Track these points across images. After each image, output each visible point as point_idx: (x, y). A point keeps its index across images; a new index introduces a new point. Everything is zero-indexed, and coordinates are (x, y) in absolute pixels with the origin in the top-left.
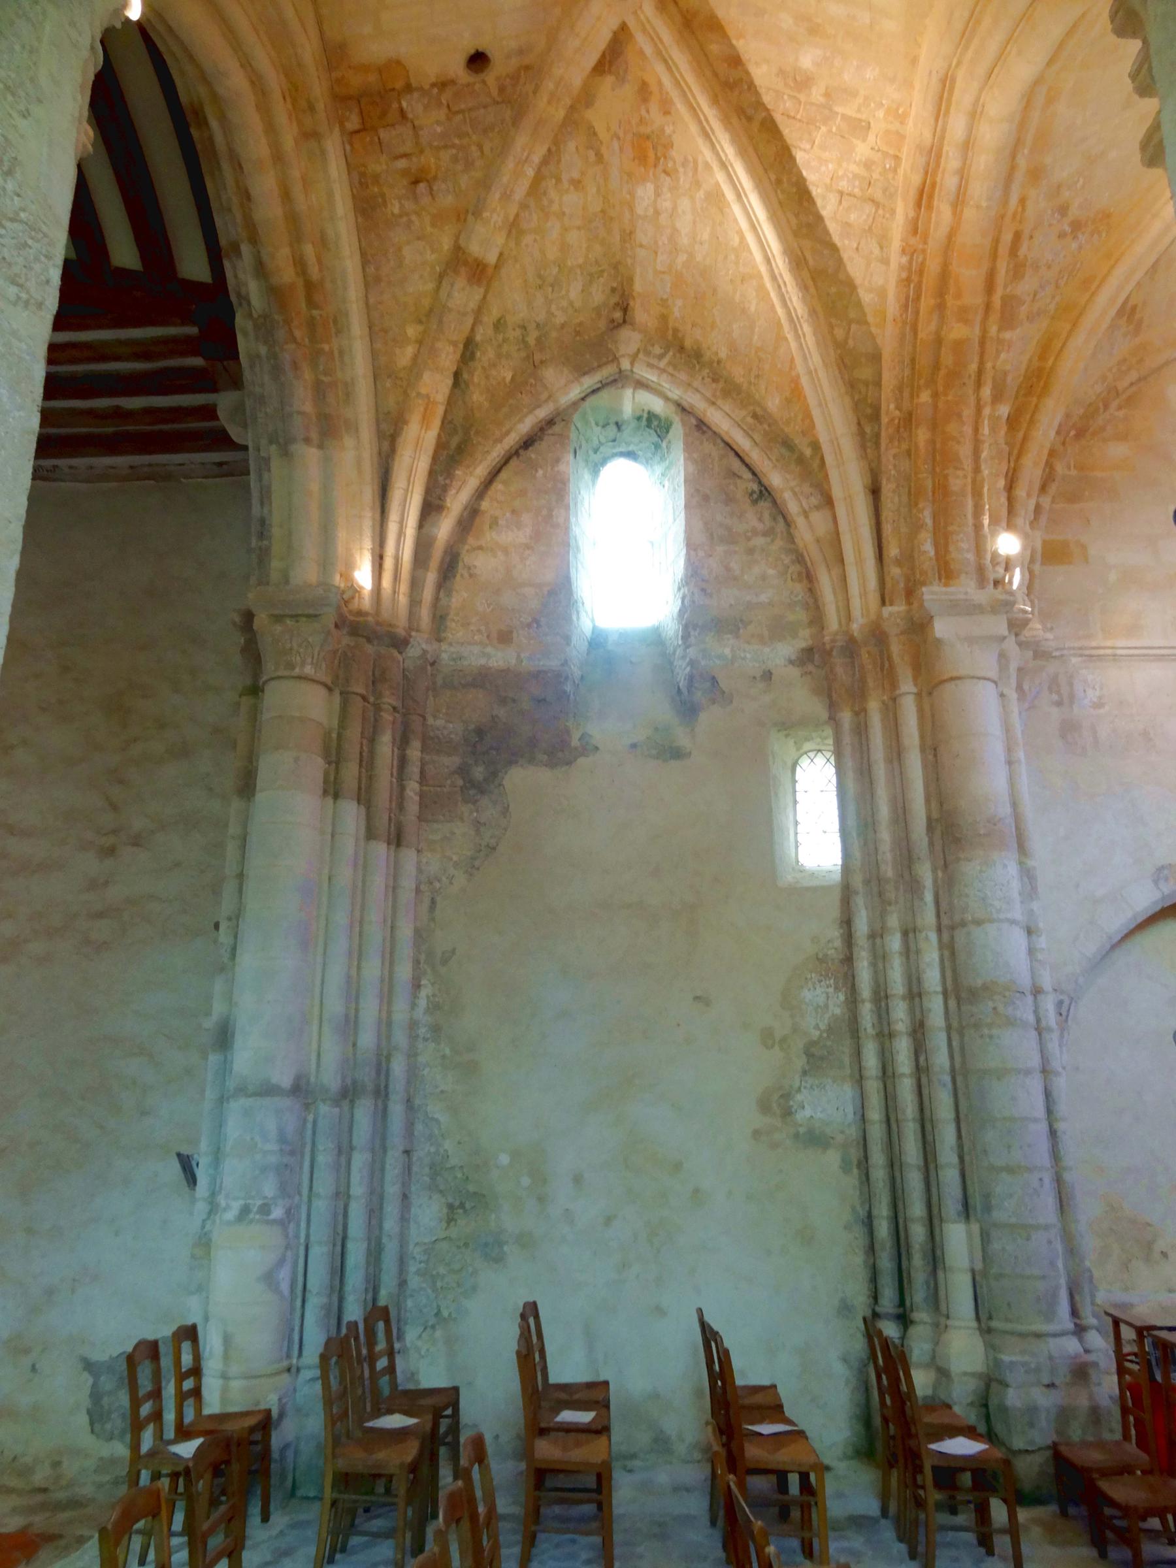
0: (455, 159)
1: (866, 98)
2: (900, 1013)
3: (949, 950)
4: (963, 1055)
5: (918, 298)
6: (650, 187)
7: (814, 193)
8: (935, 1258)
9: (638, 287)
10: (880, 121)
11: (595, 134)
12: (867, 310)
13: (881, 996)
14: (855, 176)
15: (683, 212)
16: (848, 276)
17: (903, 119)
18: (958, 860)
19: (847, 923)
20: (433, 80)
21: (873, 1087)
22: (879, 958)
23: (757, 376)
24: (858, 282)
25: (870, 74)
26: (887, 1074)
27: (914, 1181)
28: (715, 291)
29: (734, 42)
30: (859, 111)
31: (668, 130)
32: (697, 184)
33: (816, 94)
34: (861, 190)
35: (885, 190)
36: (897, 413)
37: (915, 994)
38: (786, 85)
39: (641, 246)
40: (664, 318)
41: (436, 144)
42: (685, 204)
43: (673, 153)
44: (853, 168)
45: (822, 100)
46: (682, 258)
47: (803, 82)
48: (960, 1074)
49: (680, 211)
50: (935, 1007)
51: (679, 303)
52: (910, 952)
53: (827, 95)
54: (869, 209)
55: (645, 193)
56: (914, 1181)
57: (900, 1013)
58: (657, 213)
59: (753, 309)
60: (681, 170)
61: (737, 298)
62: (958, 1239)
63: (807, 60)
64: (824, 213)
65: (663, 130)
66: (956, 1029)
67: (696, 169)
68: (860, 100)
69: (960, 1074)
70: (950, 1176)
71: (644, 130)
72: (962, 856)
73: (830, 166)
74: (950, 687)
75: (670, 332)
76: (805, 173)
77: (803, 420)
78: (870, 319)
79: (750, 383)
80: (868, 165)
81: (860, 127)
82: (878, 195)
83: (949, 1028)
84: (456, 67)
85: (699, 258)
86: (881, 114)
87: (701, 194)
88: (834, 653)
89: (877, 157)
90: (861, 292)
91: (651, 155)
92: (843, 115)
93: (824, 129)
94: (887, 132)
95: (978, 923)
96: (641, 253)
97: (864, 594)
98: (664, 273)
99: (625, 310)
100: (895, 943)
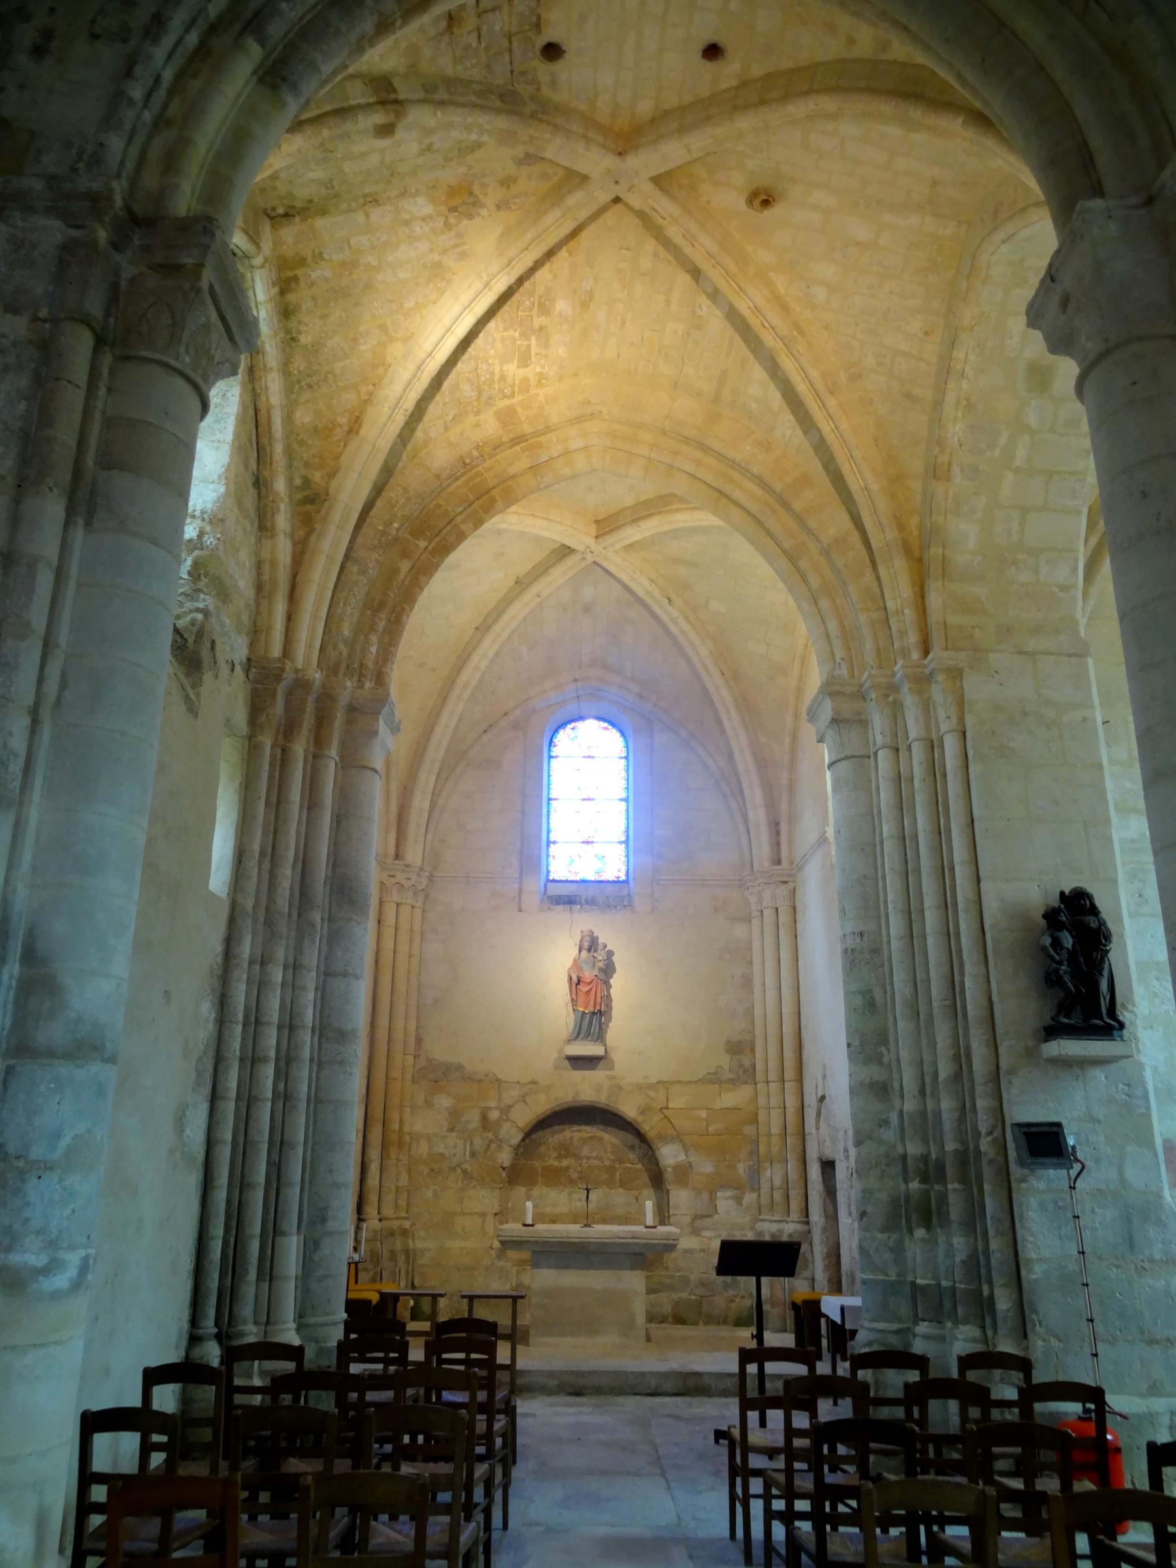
0: (468, 47)
1: (546, 356)
2: (270, 1039)
3: (322, 991)
4: (317, 1087)
5: (457, 479)
6: (429, 210)
7: (470, 349)
8: (269, 1272)
9: (320, 223)
10: (532, 371)
11: (472, 151)
12: (413, 440)
13: (255, 1021)
14: (492, 374)
15: (416, 248)
16: (426, 410)
17: (540, 384)
18: (350, 919)
19: (230, 942)
20: (544, 15)
21: (229, 1108)
22: (260, 985)
23: (310, 386)
24: (426, 419)
25: (561, 351)
26: (248, 1099)
27: (257, 1198)
28: (357, 305)
29: (564, 249)
30: (536, 354)
31: (484, 212)
32: (445, 251)
33: (538, 321)
34: (484, 383)
35: (490, 398)
36: (394, 532)
37: (289, 1026)
38: (540, 297)
39: (367, 215)
40: (302, 262)
41: (485, 27)
42: (423, 246)
43: (465, 222)
44: (497, 369)
45: (536, 326)
46: (372, 260)
47: (544, 310)
48: (317, 1100)
49: (416, 244)
50: (306, 1038)
51: (328, 274)
52: (293, 986)
53: (541, 328)
54: (474, 394)
55: (421, 206)
56: (257, 1198)
57: (270, 1039)
58: (407, 223)
59: (362, 348)
60: (453, 233)
61: (362, 328)
62: (291, 1248)
63: (561, 306)
64: (459, 364)
65: (482, 206)
66: (319, 1063)
67: (456, 246)
68: (543, 352)
69: (317, 1100)
70: (293, 1195)
71: (477, 190)
72: (355, 918)
73: (492, 352)
74: (369, 773)
75: (290, 274)
76: (481, 335)
77: (314, 455)
78: (409, 447)
79: (299, 382)
80: (503, 378)
81: (525, 361)
82: (485, 395)
83: (311, 1060)
84: (550, 34)
85: (379, 277)
86: (538, 370)
87: (436, 257)
88: (284, 683)
89: (509, 380)
90: (421, 426)
91: (456, 202)
92: (529, 346)
93: (517, 334)
94: (527, 379)
95: (345, 975)
96: (360, 217)
97: (310, 646)
98: (350, 246)
99: (286, 215)
100: (277, 975)
